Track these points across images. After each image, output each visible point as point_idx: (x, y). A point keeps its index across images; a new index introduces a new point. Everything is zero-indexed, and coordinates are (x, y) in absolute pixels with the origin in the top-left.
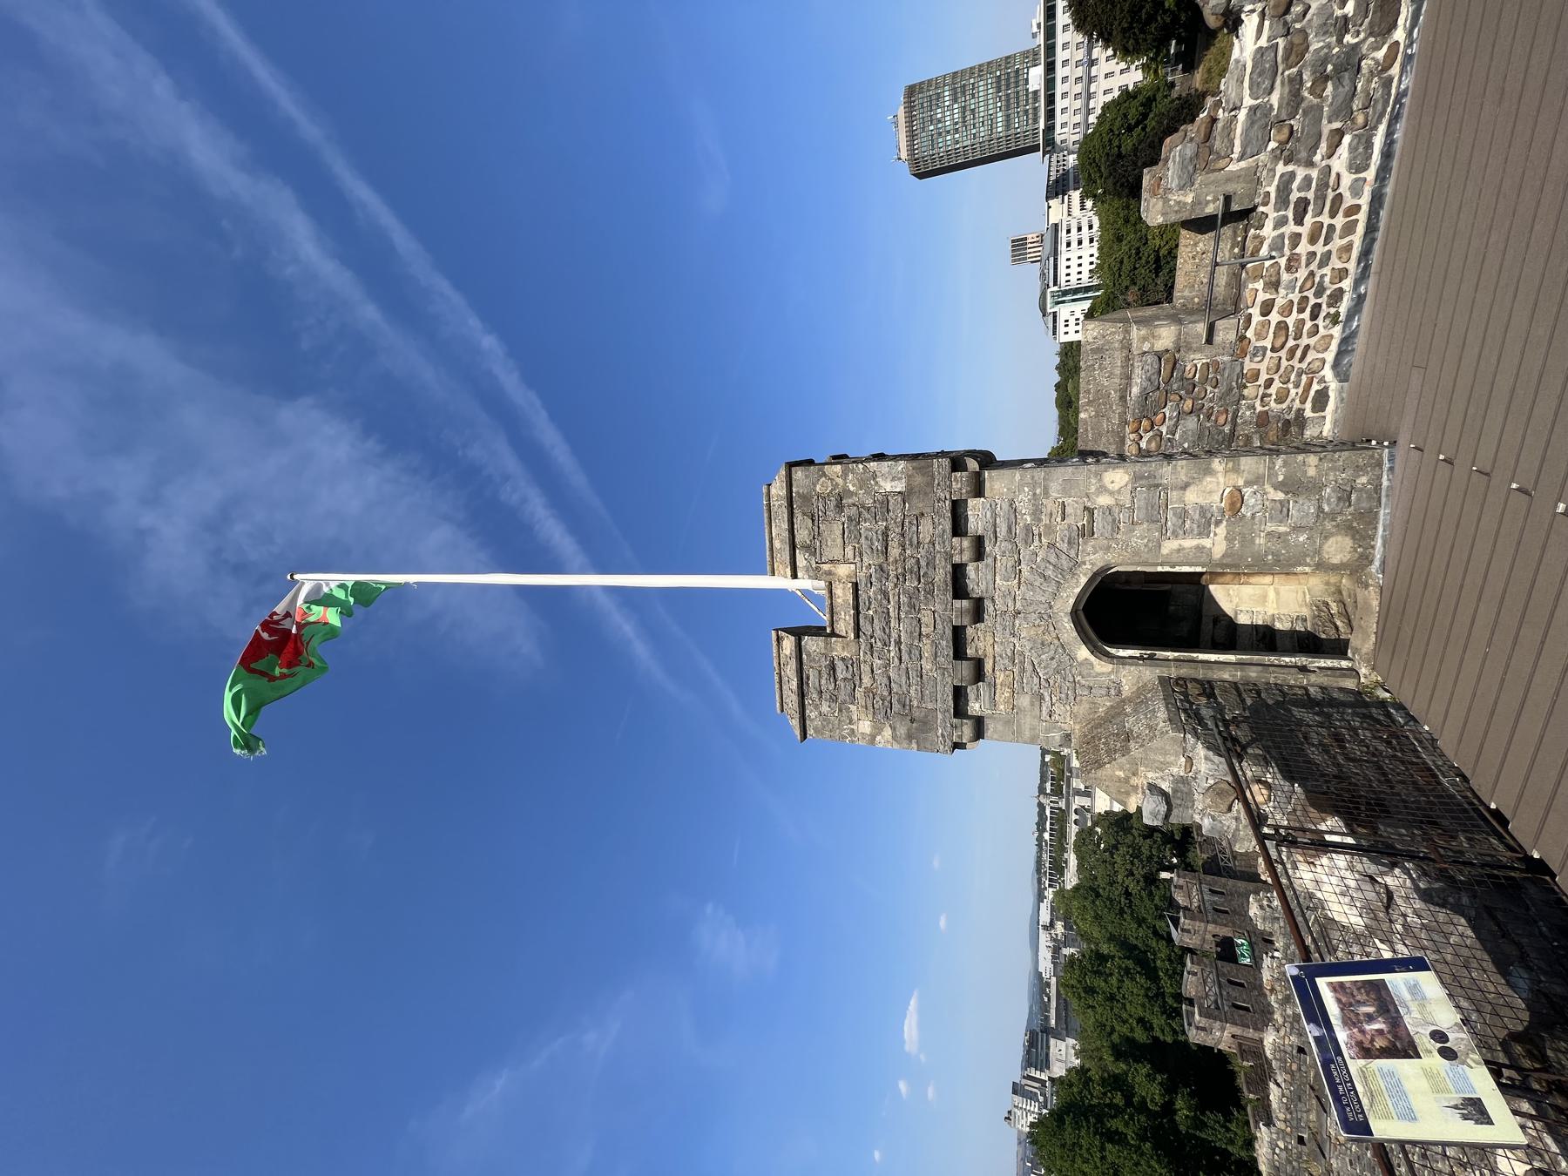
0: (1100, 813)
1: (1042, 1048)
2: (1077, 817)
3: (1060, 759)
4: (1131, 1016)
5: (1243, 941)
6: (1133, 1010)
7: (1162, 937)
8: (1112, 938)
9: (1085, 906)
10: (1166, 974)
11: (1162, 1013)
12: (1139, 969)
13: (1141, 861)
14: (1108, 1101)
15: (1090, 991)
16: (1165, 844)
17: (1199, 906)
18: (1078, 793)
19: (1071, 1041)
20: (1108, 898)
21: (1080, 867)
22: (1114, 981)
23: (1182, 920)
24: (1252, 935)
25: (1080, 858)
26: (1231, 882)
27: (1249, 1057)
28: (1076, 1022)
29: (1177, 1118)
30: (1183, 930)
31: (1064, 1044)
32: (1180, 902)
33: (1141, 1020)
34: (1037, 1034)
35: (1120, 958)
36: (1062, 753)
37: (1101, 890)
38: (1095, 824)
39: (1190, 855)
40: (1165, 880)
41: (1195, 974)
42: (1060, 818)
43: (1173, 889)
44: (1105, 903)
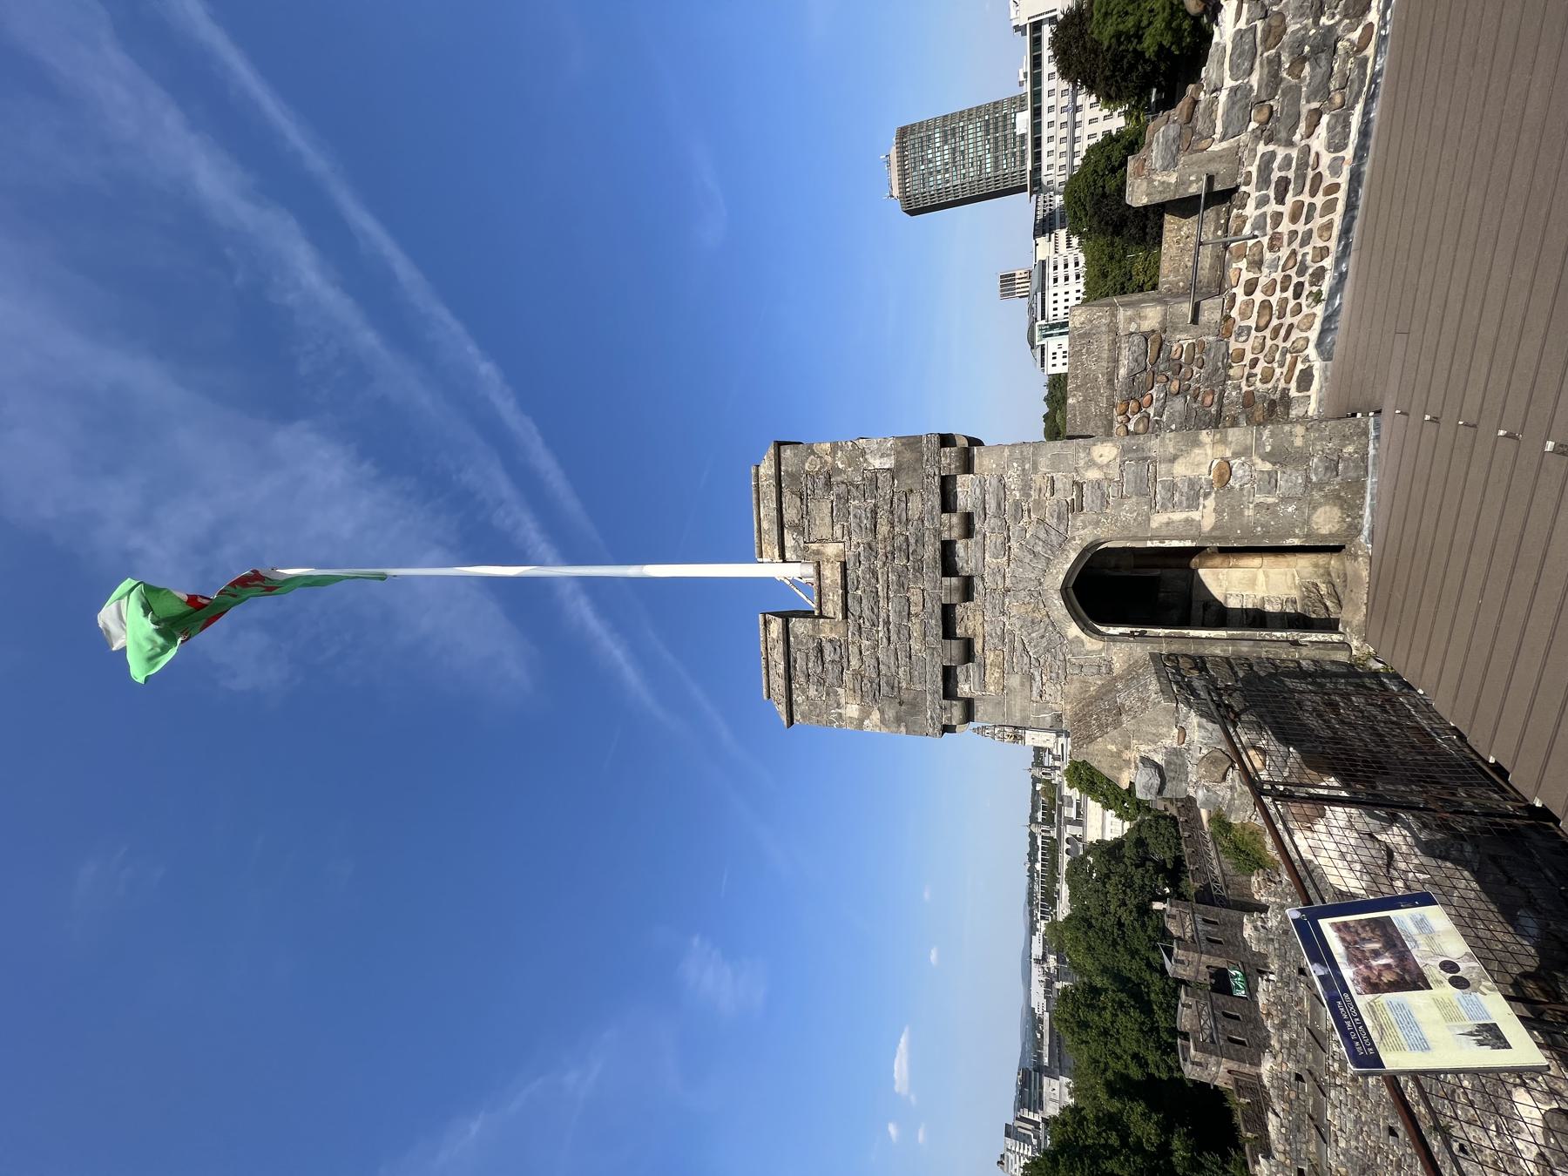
0: (1091, 842)
1: (1035, 1088)
2: (1069, 846)
3: (1052, 788)
5: (1238, 973)
6: (1128, 1045)
7: (1156, 970)
8: (1105, 970)
9: (1077, 937)
11: (1157, 1049)
12: (1133, 1003)
14: (1102, 1141)
15: (1084, 1025)
16: (1157, 873)
17: (1193, 936)
18: (1070, 821)
19: (1064, 1080)
20: (1102, 929)
22: (1107, 1015)
23: (1176, 950)
24: (1247, 966)
25: (1073, 888)
26: (1224, 912)
27: (1246, 1094)
28: (1070, 1059)
29: (1174, 1159)
30: (1176, 961)
31: (1057, 1082)
32: (1173, 932)
33: (1135, 1056)
34: (1030, 1072)
35: (1114, 991)
36: (1053, 782)
37: (1093, 921)
38: (1087, 853)
39: (1183, 884)
41: (1189, 1007)
42: (1052, 847)
43: (1166, 918)
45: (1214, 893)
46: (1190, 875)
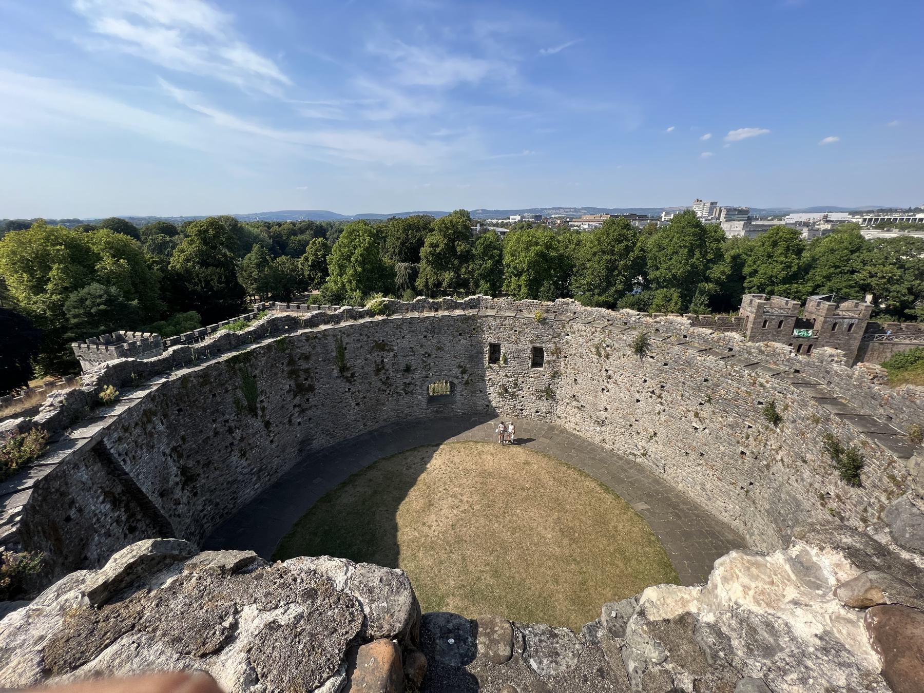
4: (758, 266)
8: (814, 259)
10: (787, 288)
11: (761, 283)
13: (885, 284)
15: (775, 244)
19: (743, 233)
20: (849, 259)
21: (884, 240)
22: (782, 258)
23: (828, 303)
25: (892, 241)
28: (755, 236)
32: (844, 304)
33: (756, 272)
35: (799, 263)
39: (888, 317)
40: (864, 297)
41: (787, 304)
44: (846, 256)
45: (877, 335)
46: (896, 323)
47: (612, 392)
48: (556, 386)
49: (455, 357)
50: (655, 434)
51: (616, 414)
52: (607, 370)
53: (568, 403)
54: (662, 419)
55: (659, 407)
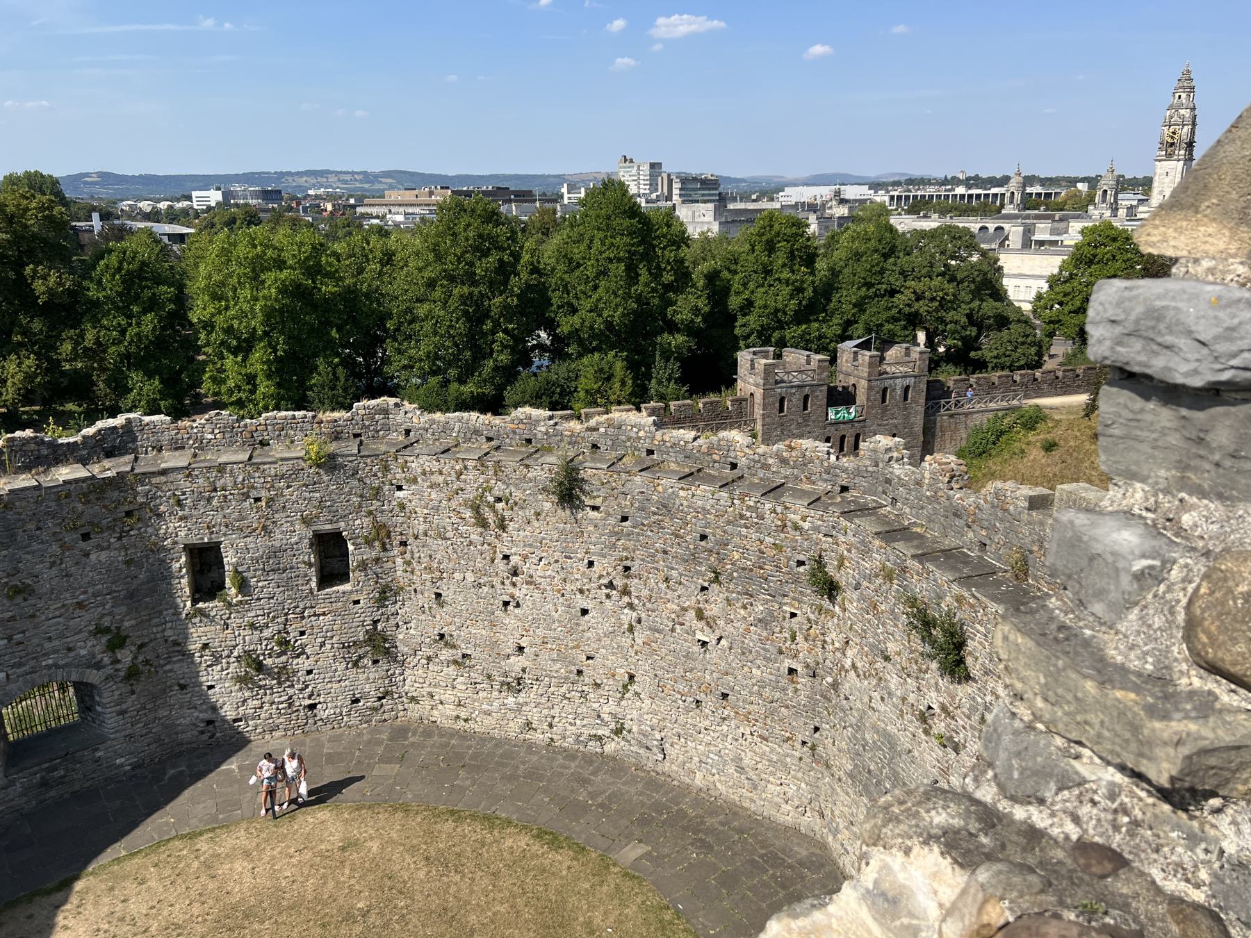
0: (999, 259)
1: (703, 195)
2: (991, 230)
3: (1082, 205)
4: (752, 292)
5: (853, 415)
6: (759, 296)
7: (845, 330)
8: (835, 273)
9: (870, 240)
10: (804, 332)
11: (762, 326)
12: (804, 303)
13: (937, 310)
14: (663, 266)
15: (771, 248)
16: (963, 339)
17: (887, 373)
18: (1028, 231)
19: (715, 228)
21: (922, 234)
22: (786, 274)
23: (868, 353)
24: (862, 424)
25: (932, 235)
26: (921, 409)
27: (736, 407)
28: (738, 233)
29: (666, 335)
30: (855, 353)
31: (712, 219)
32: (889, 353)
33: (749, 304)
34: (717, 189)
35: (813, 282)
36: (1091, 208)
37: (892, 260)
38: (984, 254)
39: (950, 368)
40: (915, 337)
41: (808, 362)
42: (989, 207)
43: (905, 345)
44: (877, 264)
45: (943, 402)
46: (963, 376)
47: (527, 604)
48: (392, 622)
49: (80, 605)
50: (631, 677)
51: (544, 656)
52: (506, 557)
53: (429, 659)
54: (639, 641)
55: (628, 616)
